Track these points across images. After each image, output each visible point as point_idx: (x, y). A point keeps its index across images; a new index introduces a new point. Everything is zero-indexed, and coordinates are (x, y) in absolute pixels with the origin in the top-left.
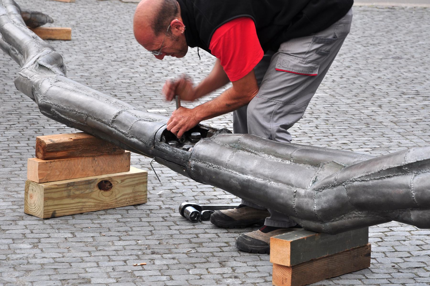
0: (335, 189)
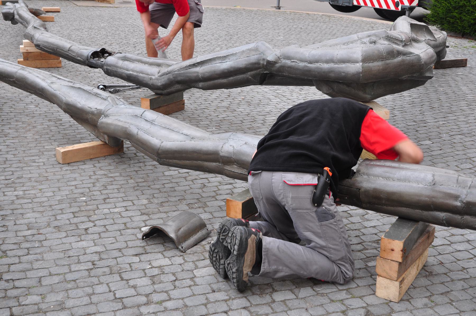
0: (167, 75)
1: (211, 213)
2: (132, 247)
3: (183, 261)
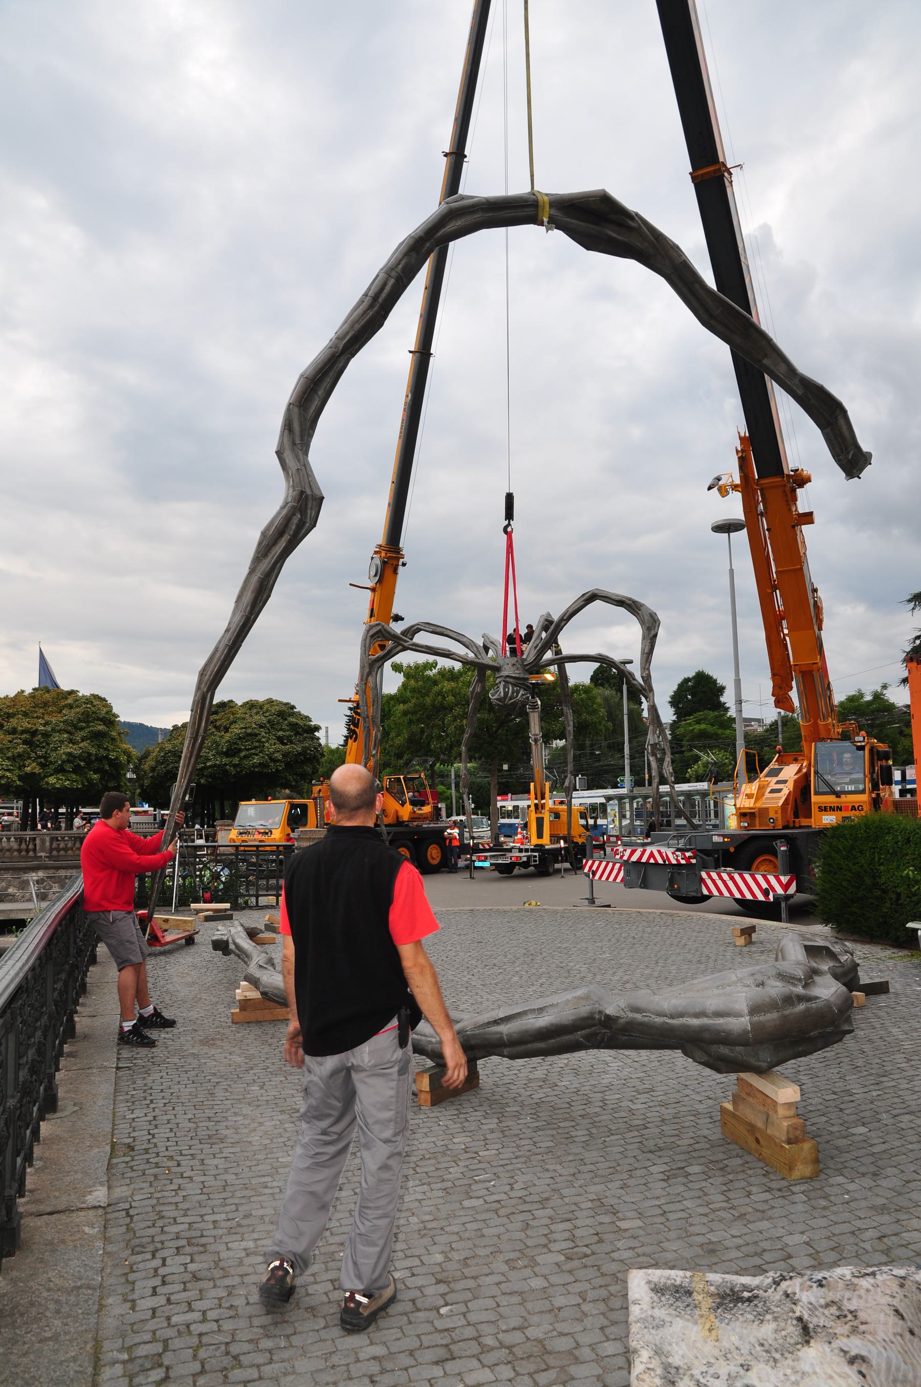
1: (545, 1277)
2: (429, 1347)
3: (512, 1374)
